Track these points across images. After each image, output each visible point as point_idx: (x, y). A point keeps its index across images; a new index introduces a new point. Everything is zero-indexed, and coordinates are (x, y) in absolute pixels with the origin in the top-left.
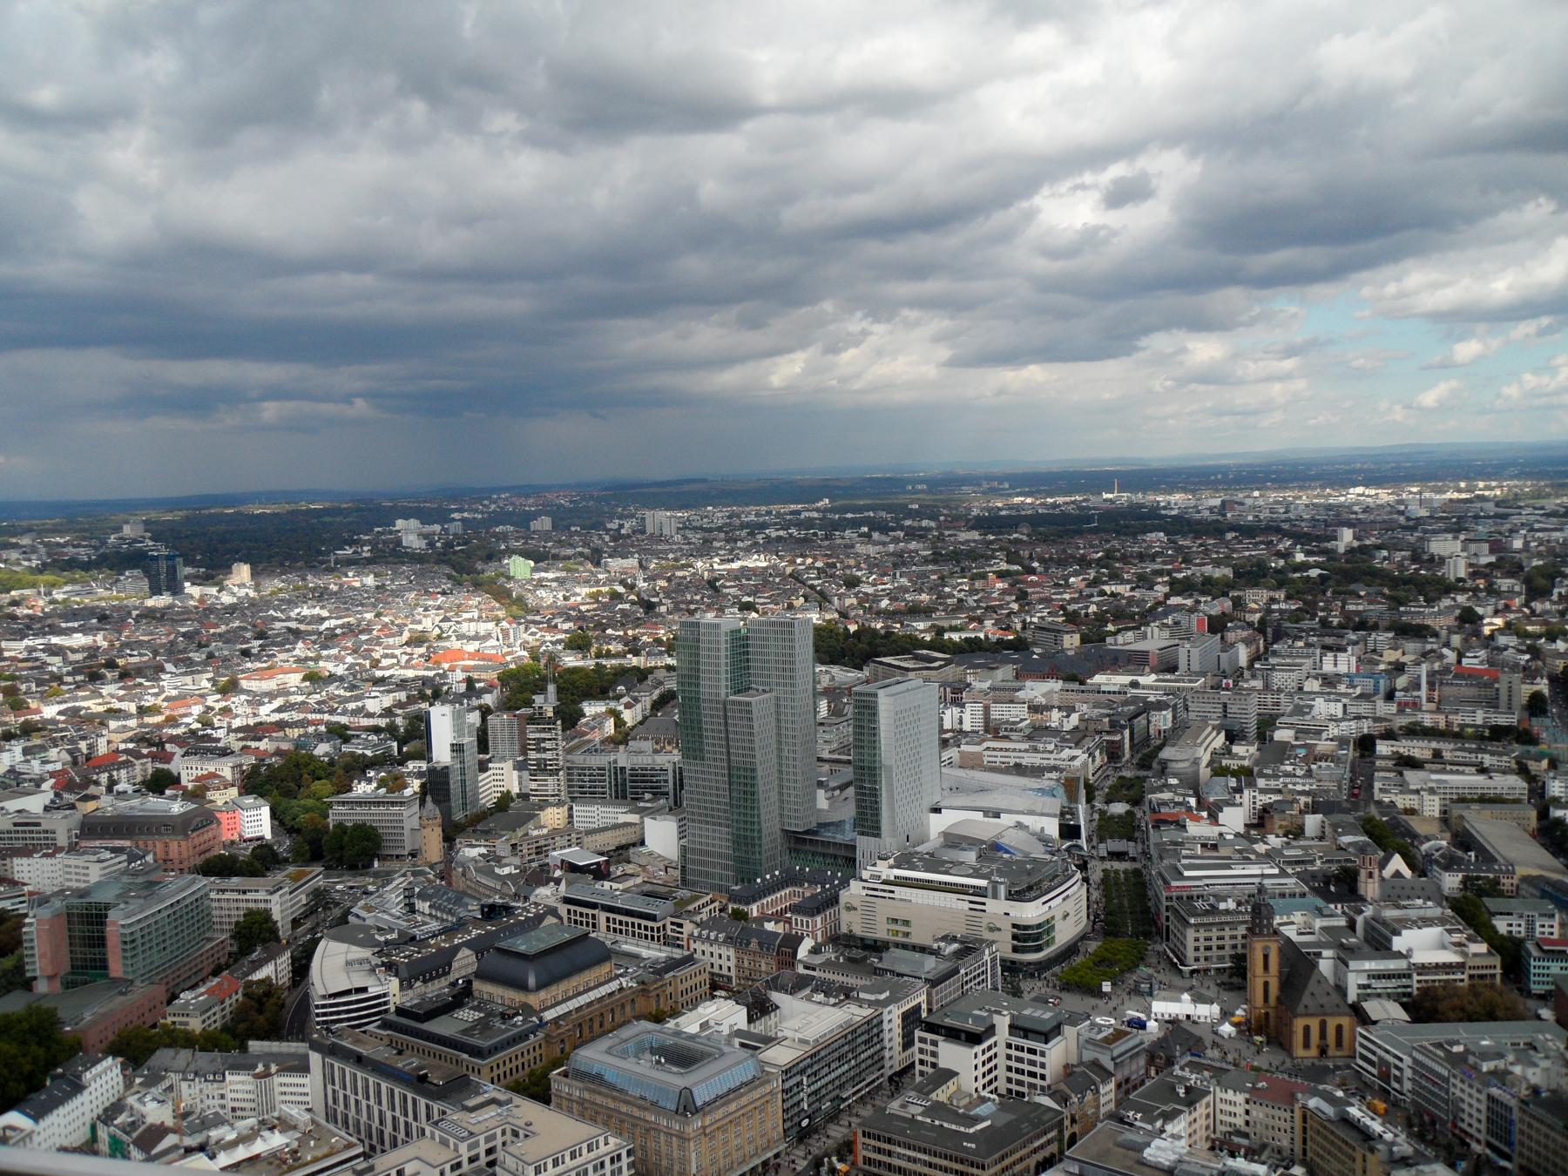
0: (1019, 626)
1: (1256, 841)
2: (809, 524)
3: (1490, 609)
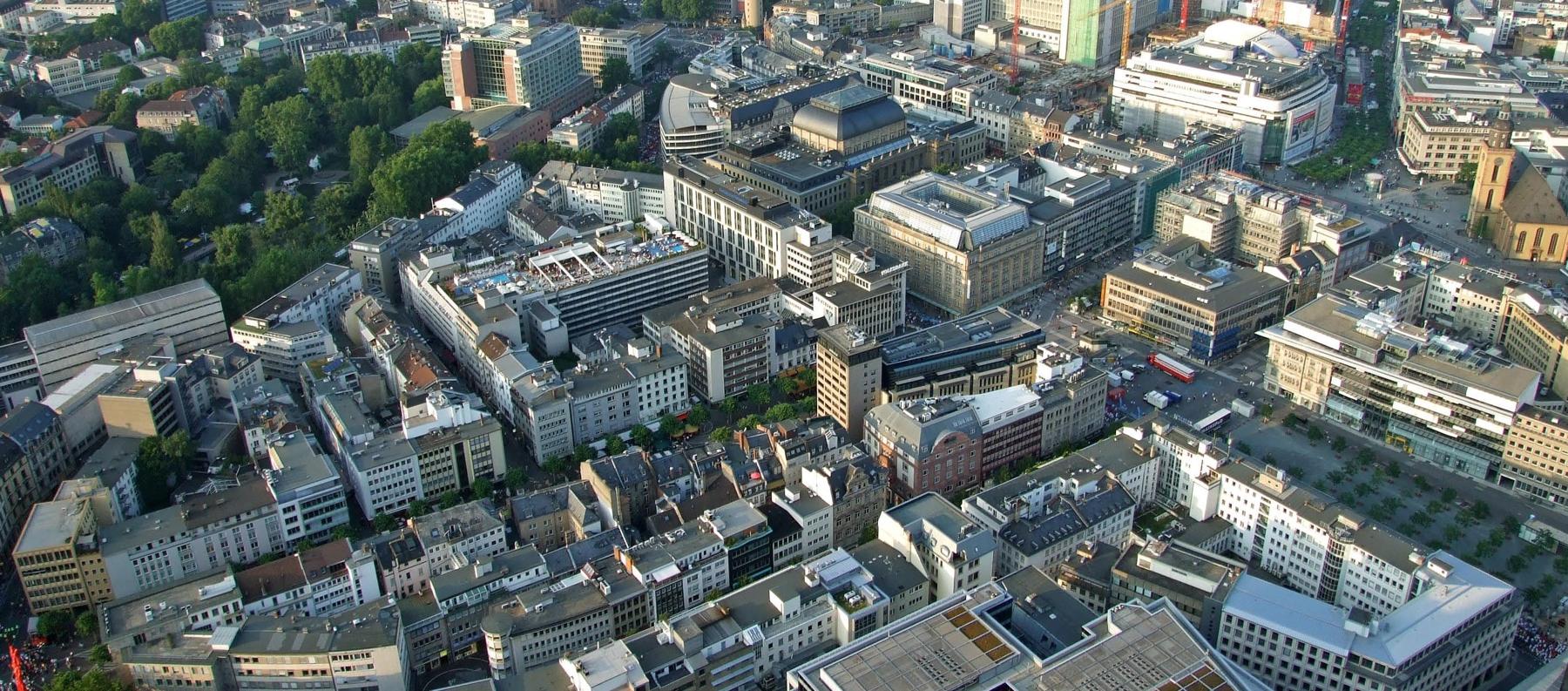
1: (1502, 62)
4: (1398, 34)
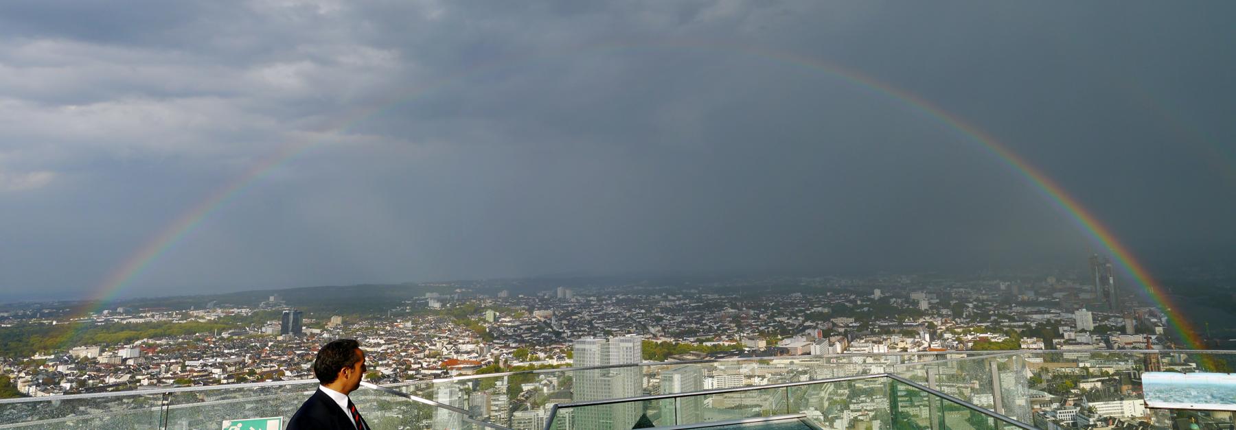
0: (738, 338)
3: (940, 323)
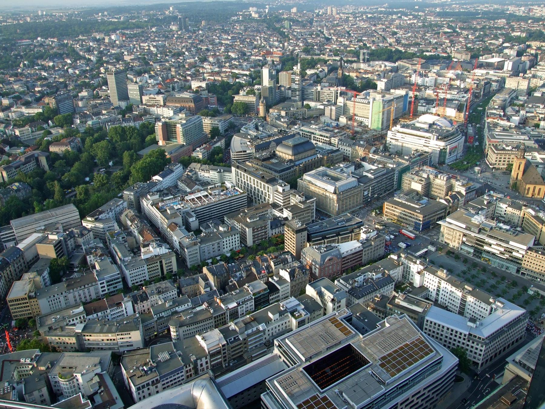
2: (381, 12)
4: (486, 119)
